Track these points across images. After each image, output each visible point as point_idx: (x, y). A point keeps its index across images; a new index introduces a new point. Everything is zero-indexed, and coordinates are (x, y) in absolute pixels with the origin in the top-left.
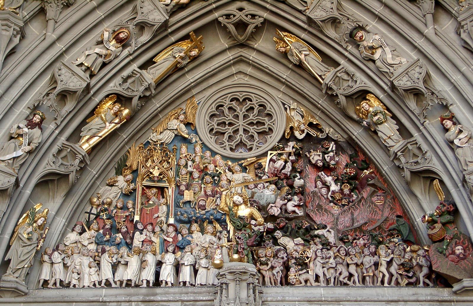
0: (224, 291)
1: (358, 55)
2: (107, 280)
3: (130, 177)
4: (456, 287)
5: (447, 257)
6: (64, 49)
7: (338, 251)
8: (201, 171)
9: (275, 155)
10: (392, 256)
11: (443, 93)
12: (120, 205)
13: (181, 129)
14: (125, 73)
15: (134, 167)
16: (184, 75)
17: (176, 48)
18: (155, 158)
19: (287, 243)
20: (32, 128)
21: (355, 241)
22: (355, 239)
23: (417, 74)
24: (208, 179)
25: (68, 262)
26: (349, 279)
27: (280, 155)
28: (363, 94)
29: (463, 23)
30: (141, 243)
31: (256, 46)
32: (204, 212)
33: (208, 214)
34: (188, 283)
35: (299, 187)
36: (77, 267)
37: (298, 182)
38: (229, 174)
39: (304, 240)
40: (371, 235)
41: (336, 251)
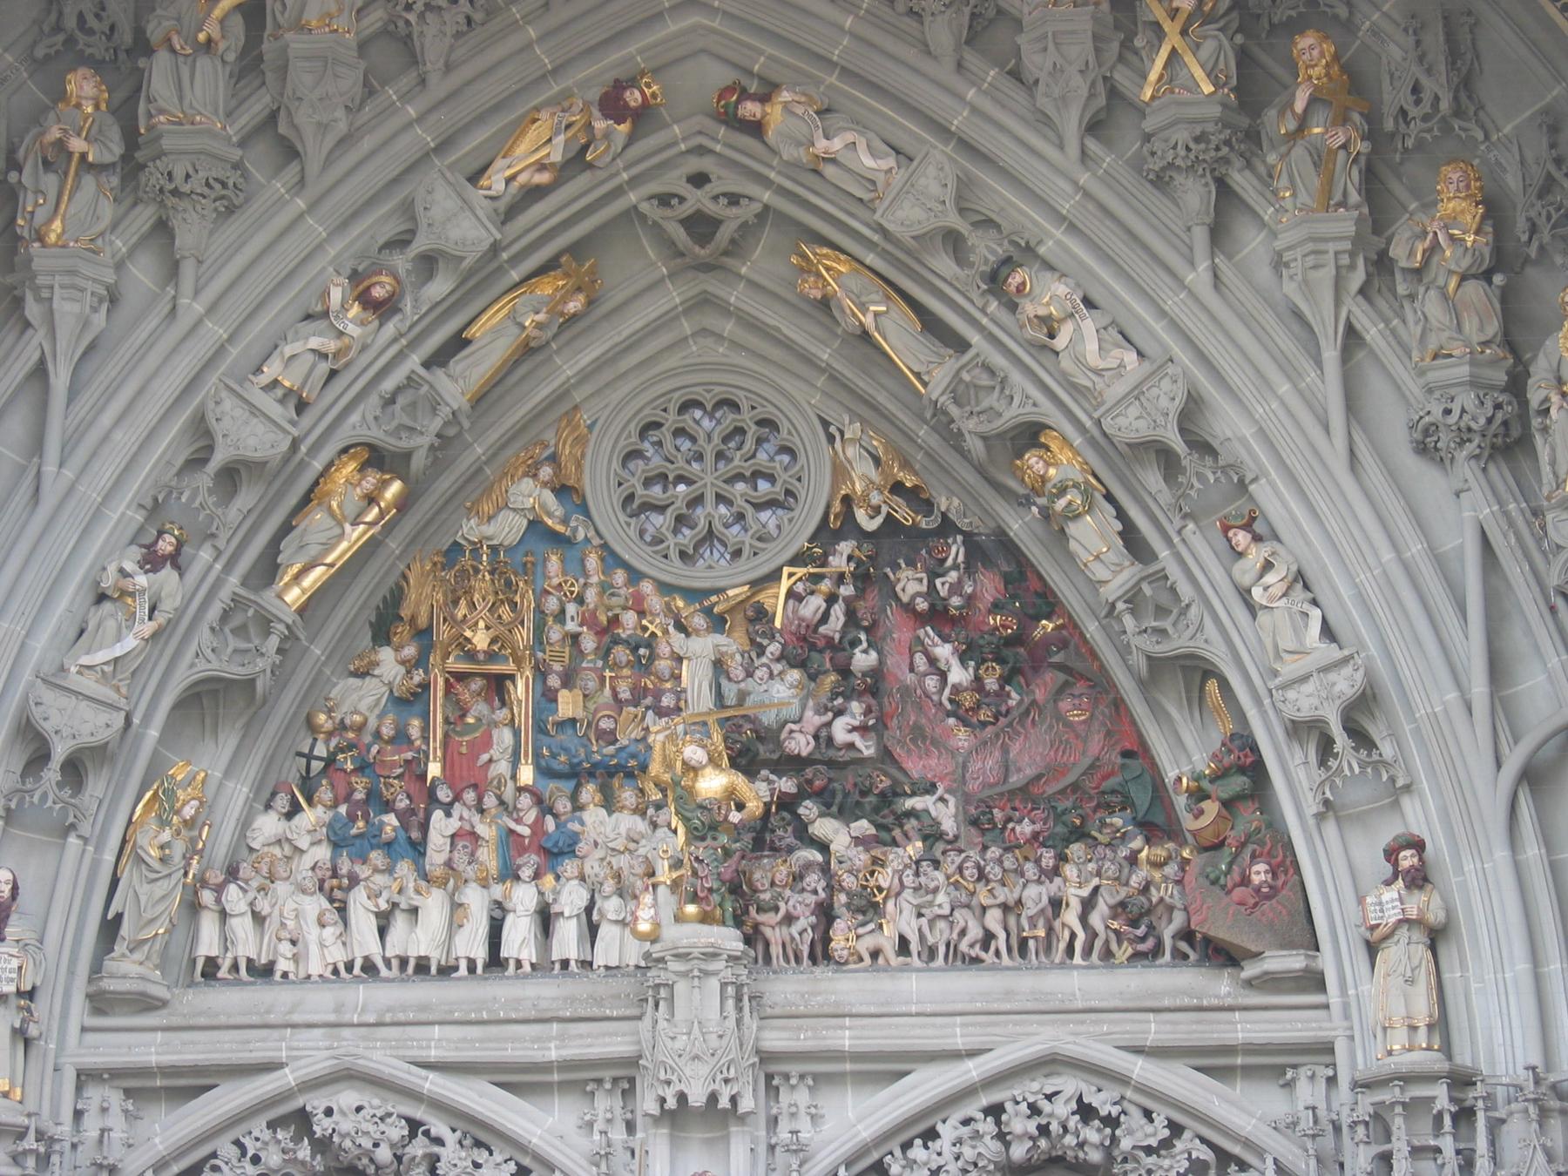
0: (662, 1003)
1: (1015, 330)
2: (366, 959)
3: (410, 651)
4: (1250, 970)
5: (1229, 892)
6: (225, 336)
7: (960, 869)
8: (601, 632)
9: (800, 579)
10: (1096, 881)
11: (1237, 445)
12: (387, 731)
13: (543, 506)
14: (388, 385)
15: (422, 621)
16: (550, 359)
17: (522, 299)
18: (476, 597)
19: (831, 837)
20: (155, 570)
21: (1010, 825)
22: (1010, 819)
23: (1167, 398)
24: (621, 654)
25: (264, 906)
26: (986, 948)
27: (816, 578)
28: (1030, 435)
29: (1287, 257)
30: (448, 841)
31: (744, 270)
32: (611, 749)
33: (624, 755)
34: (573, 963)
35: (864, 674)
36: (288, 922)
37: (863, 660)
38: (677, 638)
39: (878, 826)
40: (1054, 808)
41: (951, 869)
